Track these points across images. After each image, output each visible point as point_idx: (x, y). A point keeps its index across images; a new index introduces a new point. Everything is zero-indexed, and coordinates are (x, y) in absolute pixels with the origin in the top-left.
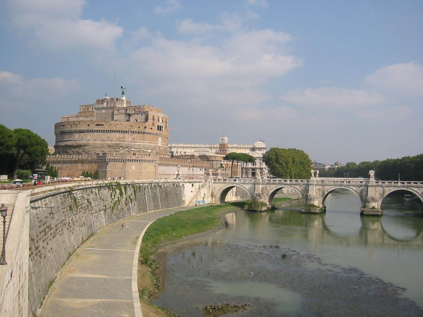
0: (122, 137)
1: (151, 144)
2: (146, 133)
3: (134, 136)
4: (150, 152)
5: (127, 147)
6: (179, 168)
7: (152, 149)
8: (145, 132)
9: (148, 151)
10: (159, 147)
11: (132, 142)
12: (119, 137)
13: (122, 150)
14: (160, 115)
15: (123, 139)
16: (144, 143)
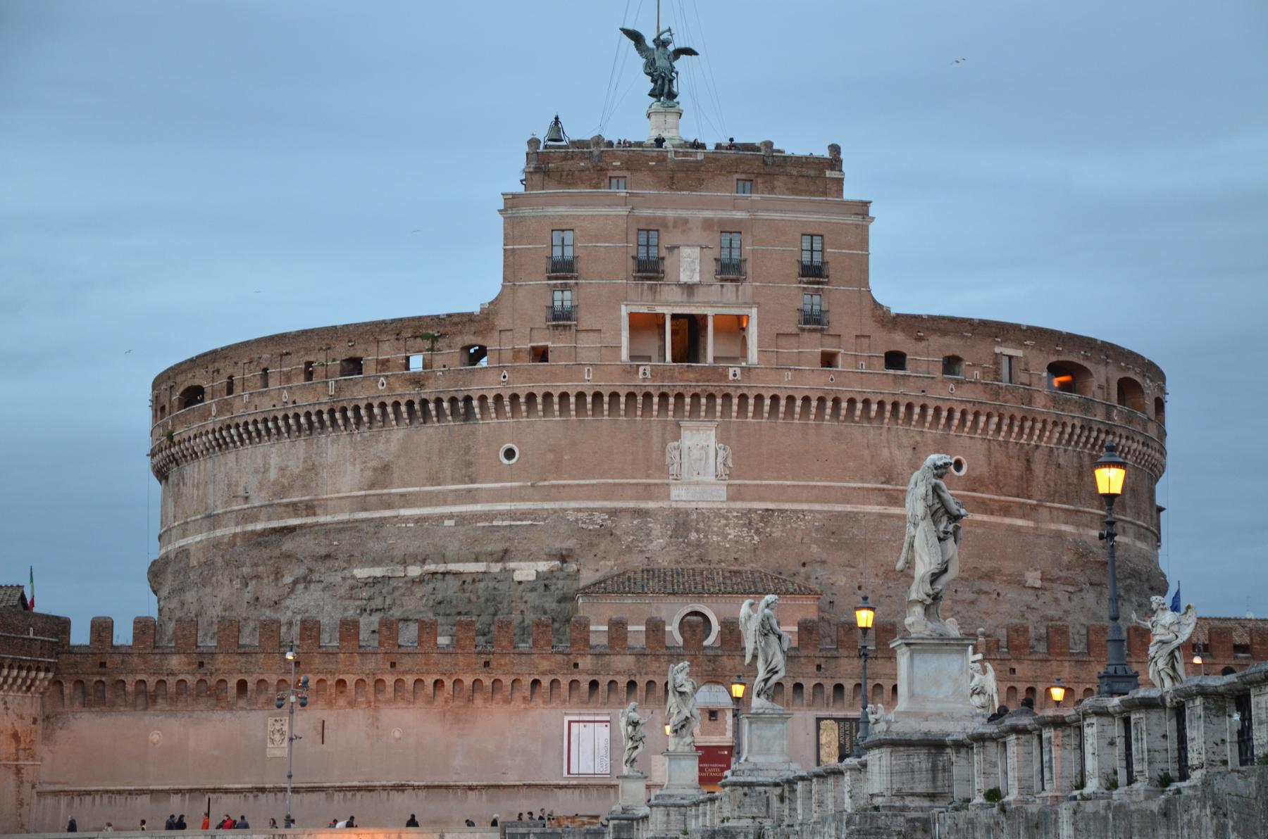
0: (297, 471)
1: (549, 505)
2: (483, 399)
3: (381, 447)
4: (532, 577)
5: (323, 551)
7: (570, 543)
8: (468, 399)
9: (518, 576)
10: (681, 523)
11: (363, 504)
12: (281, 469)
13: (301, 587)
14: (670, 213)
15: (304, 486)
16: (471, 497)
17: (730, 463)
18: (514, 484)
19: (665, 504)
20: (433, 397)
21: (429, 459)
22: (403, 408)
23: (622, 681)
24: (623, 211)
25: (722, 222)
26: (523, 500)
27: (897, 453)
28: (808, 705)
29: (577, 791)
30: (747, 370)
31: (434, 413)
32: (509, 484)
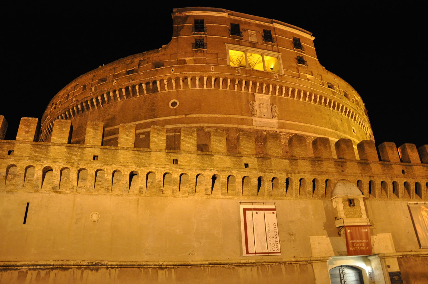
2: (162, 81)
3: (112, 110)
6: (340, 206)
8: (155, 82)
17: (277, 111)
18: (177, 117)
19: (251, 127)
20: (138, 83)
21: (134, 111)
22: (124, 90)
23: (282, 178)
24: (225, 15)
25: (262, 26)
26: (181, 123)
27: (337, 120)
28: (403, 197)
29: (255, 269)
30: (280, 76)
31: (137, 90)
32: (173, 117)
